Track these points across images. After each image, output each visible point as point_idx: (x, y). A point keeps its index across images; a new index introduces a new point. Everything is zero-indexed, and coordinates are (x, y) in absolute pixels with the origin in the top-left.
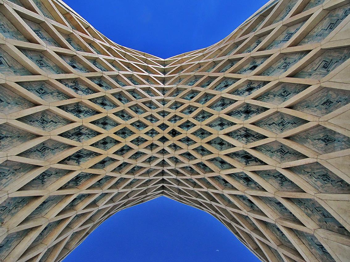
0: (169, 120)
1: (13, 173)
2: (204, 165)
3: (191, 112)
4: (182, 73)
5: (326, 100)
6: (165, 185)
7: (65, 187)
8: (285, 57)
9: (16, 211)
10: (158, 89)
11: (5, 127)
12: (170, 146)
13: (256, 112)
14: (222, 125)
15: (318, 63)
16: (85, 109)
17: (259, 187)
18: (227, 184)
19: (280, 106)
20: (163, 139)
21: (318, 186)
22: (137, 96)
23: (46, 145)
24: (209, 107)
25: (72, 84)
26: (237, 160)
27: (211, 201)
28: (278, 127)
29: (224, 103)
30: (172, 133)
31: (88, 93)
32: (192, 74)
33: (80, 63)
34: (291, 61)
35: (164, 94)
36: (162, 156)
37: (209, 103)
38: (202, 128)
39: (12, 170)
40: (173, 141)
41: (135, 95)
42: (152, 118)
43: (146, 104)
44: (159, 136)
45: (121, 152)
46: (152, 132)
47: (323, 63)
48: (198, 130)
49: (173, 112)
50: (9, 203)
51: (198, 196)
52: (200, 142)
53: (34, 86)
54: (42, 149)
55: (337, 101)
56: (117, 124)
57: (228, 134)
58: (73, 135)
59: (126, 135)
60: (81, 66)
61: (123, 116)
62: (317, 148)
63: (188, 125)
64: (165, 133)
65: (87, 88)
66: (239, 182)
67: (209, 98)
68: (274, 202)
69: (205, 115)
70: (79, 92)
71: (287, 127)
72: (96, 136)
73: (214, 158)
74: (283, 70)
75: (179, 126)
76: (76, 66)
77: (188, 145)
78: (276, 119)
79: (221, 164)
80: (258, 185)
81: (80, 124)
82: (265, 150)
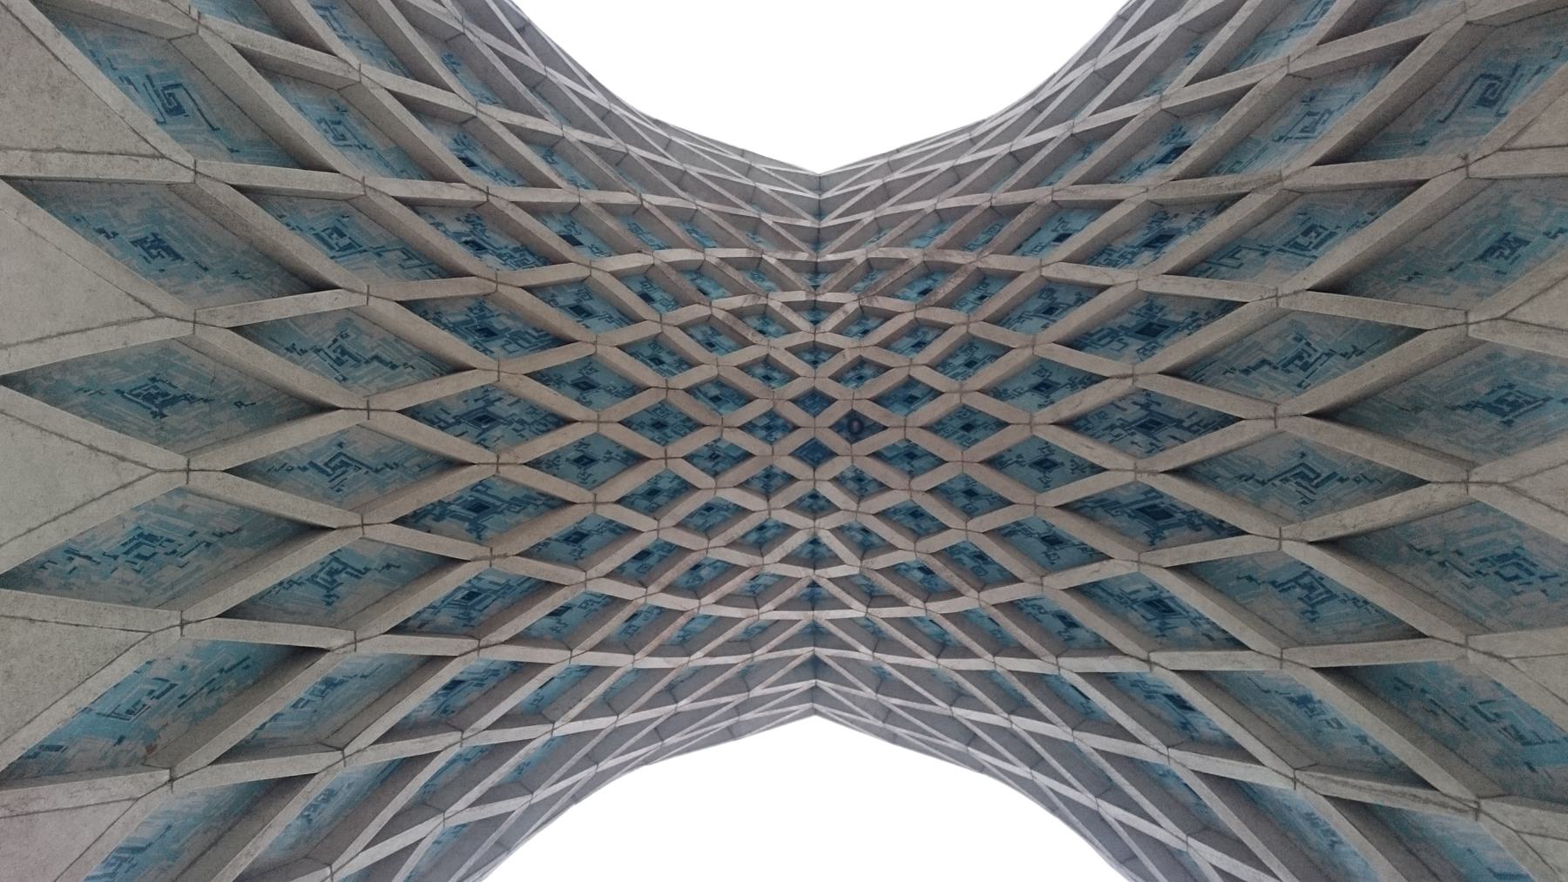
0: (838, 377)
1: (208, 545)
2: (981, 557)
3: (920, 345)
4: (887, 209)
5: (1494, 237)
6: (824, 653)
7: (420, 626)
8: (1307, 92)
10: (796, 266)
11: (182, 359)
12: (838, 480)
13: (1187, 327)
14: (1045, 388)
15: (1457, 87)
16: (510, 323)
17: (1215, 635)
18: (1075, 632)
19: (1286, 288)
21: (1477, 607)
22: (710, 290)
23: (349, 450)
24: (999, 320)
26: (1112, 528)
27: (1011, 713)
28: (1283, 377)
29: (1050, 300)
30: (849, 427)
31: (522, 264)
32: (927, 205)
34: (1333, 101)
35: (815, 287)
36: (810, 523)
37: (993, 306)
38: (964, 406)
39: (203, 535)
41: (706, 285)
42: (769, 370)
43: (748, 321)
44: (797, 440)
45: (652, 499)
46: (773, 426)
47: (1478, 89)
48: (951, 416)
49: (850, 348)
50: (184, 668)
51: (958, 696)
52: (959, 461)
53: (309, 215)
54: (336, 468)
55: (1547, 234)
56: (635, 389)
57: (1071, 424)
58: (458, 420)
59: (668, 431)
60: (495, 164)
61: (657, 361)
62: (1463, 442)
63: (909, 394)
66: (1126, 620)
67: (991, 289)
68: (1278, 697)
69: (979, 355)
70: (490, 259)
71: (1327, 371)
72: (549, 431)
73: (1017, 523)
74: (1301, 144)
75: (877, 400)
76: (476, 160)
77: (910, 472)
78: (1275, 346)
79: (1045, 548)
80: (1207, 626)
81: (490, 378)
82: (1229, 476)
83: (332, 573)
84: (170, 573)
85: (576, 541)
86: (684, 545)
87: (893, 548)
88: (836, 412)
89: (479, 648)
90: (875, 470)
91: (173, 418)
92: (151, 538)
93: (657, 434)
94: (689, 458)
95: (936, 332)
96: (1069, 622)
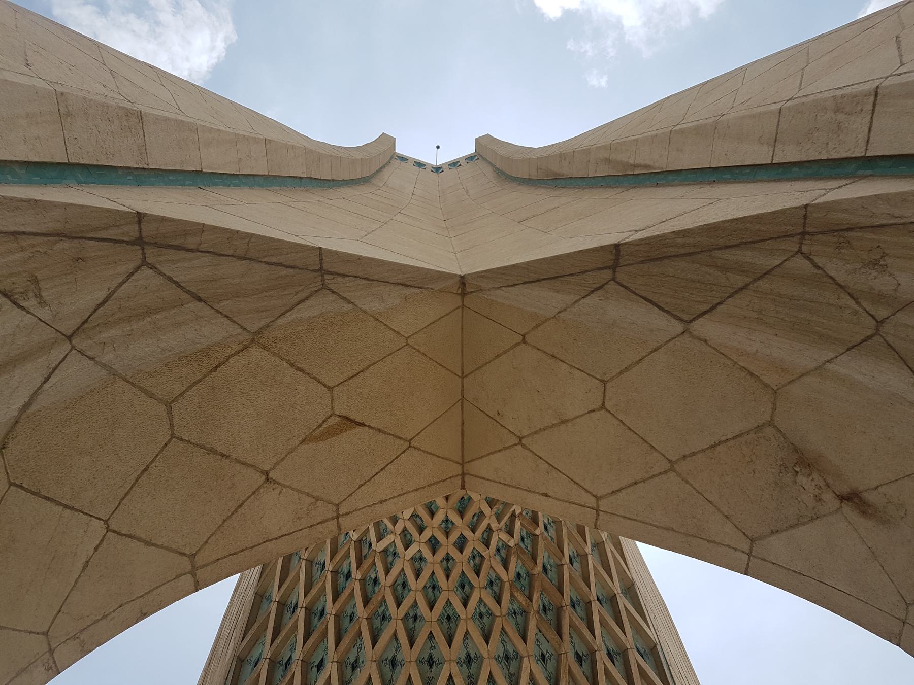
44: (441, 537)
48: (454, 609)
52: (431, 618)
64: (447, 546)
67: (519, 617)
69: (485, 619)
79: (390, 658)
87: (387, 572)
88: (454, 553)
95: (497, 592)
96: (355, 666)
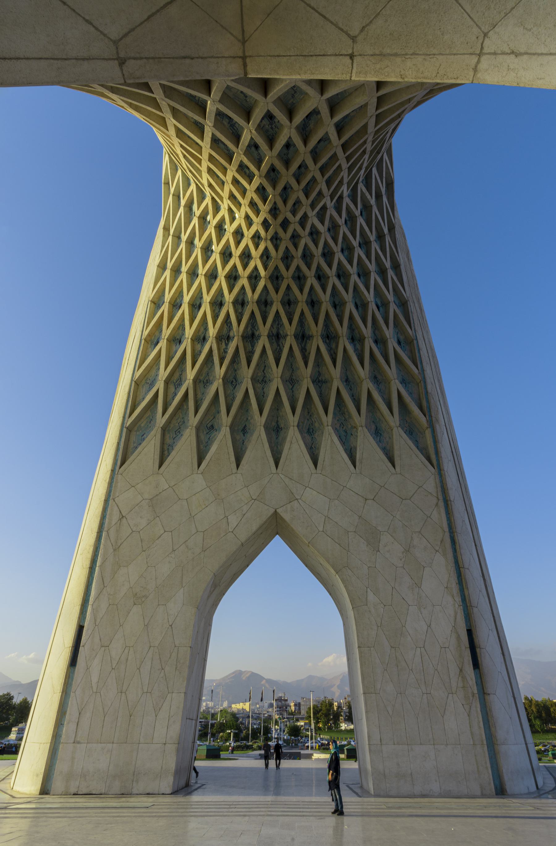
9: (347, 413)
16: (249, 329)
20: (285, 224)
25: (224, 344)
31: (231, 323)
33: (199, 331)
40: (286, 212)
58: (278, 345)
59: (279, 275)
65: (225, 324)
70: (231, 334)
76: (203, 335)
83: (319, 382)
84: (317, 425)
85: (314, 303)
86: (316, 266)
89: (343, 336)
90: (290, 203)
91: (282, 426)
92: (309, 429)
93: (280, 279)
94: (287, 268)
